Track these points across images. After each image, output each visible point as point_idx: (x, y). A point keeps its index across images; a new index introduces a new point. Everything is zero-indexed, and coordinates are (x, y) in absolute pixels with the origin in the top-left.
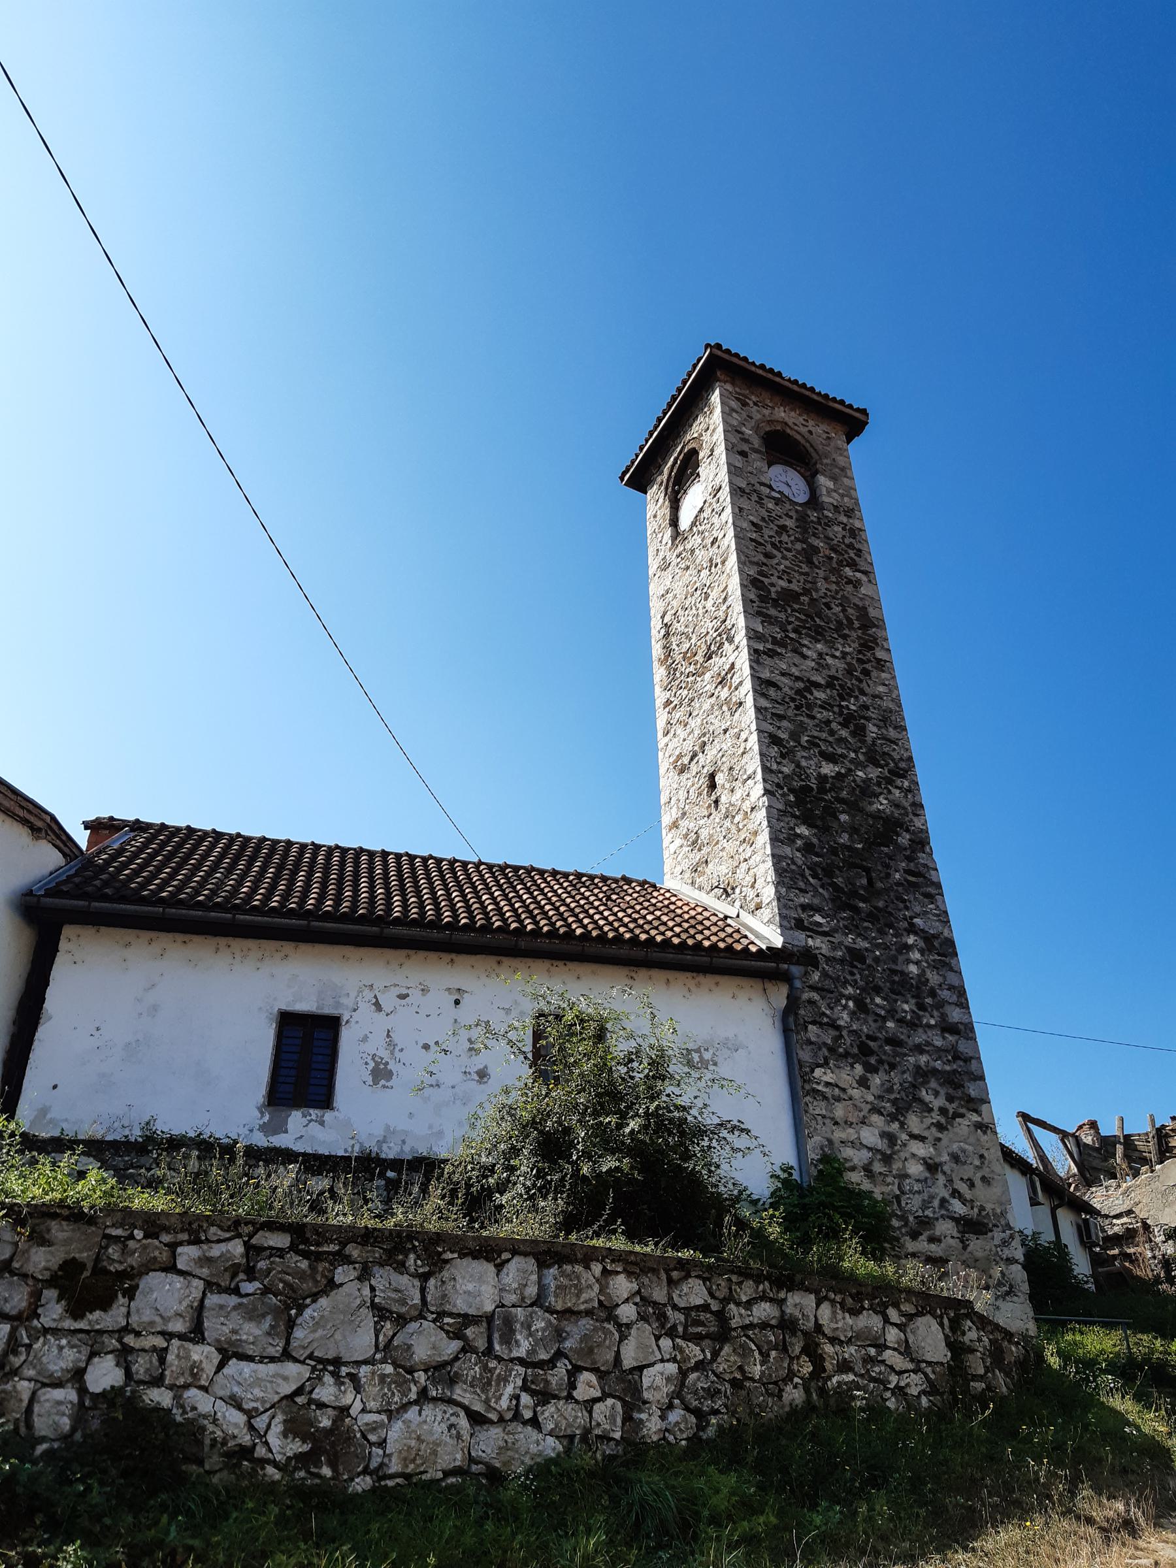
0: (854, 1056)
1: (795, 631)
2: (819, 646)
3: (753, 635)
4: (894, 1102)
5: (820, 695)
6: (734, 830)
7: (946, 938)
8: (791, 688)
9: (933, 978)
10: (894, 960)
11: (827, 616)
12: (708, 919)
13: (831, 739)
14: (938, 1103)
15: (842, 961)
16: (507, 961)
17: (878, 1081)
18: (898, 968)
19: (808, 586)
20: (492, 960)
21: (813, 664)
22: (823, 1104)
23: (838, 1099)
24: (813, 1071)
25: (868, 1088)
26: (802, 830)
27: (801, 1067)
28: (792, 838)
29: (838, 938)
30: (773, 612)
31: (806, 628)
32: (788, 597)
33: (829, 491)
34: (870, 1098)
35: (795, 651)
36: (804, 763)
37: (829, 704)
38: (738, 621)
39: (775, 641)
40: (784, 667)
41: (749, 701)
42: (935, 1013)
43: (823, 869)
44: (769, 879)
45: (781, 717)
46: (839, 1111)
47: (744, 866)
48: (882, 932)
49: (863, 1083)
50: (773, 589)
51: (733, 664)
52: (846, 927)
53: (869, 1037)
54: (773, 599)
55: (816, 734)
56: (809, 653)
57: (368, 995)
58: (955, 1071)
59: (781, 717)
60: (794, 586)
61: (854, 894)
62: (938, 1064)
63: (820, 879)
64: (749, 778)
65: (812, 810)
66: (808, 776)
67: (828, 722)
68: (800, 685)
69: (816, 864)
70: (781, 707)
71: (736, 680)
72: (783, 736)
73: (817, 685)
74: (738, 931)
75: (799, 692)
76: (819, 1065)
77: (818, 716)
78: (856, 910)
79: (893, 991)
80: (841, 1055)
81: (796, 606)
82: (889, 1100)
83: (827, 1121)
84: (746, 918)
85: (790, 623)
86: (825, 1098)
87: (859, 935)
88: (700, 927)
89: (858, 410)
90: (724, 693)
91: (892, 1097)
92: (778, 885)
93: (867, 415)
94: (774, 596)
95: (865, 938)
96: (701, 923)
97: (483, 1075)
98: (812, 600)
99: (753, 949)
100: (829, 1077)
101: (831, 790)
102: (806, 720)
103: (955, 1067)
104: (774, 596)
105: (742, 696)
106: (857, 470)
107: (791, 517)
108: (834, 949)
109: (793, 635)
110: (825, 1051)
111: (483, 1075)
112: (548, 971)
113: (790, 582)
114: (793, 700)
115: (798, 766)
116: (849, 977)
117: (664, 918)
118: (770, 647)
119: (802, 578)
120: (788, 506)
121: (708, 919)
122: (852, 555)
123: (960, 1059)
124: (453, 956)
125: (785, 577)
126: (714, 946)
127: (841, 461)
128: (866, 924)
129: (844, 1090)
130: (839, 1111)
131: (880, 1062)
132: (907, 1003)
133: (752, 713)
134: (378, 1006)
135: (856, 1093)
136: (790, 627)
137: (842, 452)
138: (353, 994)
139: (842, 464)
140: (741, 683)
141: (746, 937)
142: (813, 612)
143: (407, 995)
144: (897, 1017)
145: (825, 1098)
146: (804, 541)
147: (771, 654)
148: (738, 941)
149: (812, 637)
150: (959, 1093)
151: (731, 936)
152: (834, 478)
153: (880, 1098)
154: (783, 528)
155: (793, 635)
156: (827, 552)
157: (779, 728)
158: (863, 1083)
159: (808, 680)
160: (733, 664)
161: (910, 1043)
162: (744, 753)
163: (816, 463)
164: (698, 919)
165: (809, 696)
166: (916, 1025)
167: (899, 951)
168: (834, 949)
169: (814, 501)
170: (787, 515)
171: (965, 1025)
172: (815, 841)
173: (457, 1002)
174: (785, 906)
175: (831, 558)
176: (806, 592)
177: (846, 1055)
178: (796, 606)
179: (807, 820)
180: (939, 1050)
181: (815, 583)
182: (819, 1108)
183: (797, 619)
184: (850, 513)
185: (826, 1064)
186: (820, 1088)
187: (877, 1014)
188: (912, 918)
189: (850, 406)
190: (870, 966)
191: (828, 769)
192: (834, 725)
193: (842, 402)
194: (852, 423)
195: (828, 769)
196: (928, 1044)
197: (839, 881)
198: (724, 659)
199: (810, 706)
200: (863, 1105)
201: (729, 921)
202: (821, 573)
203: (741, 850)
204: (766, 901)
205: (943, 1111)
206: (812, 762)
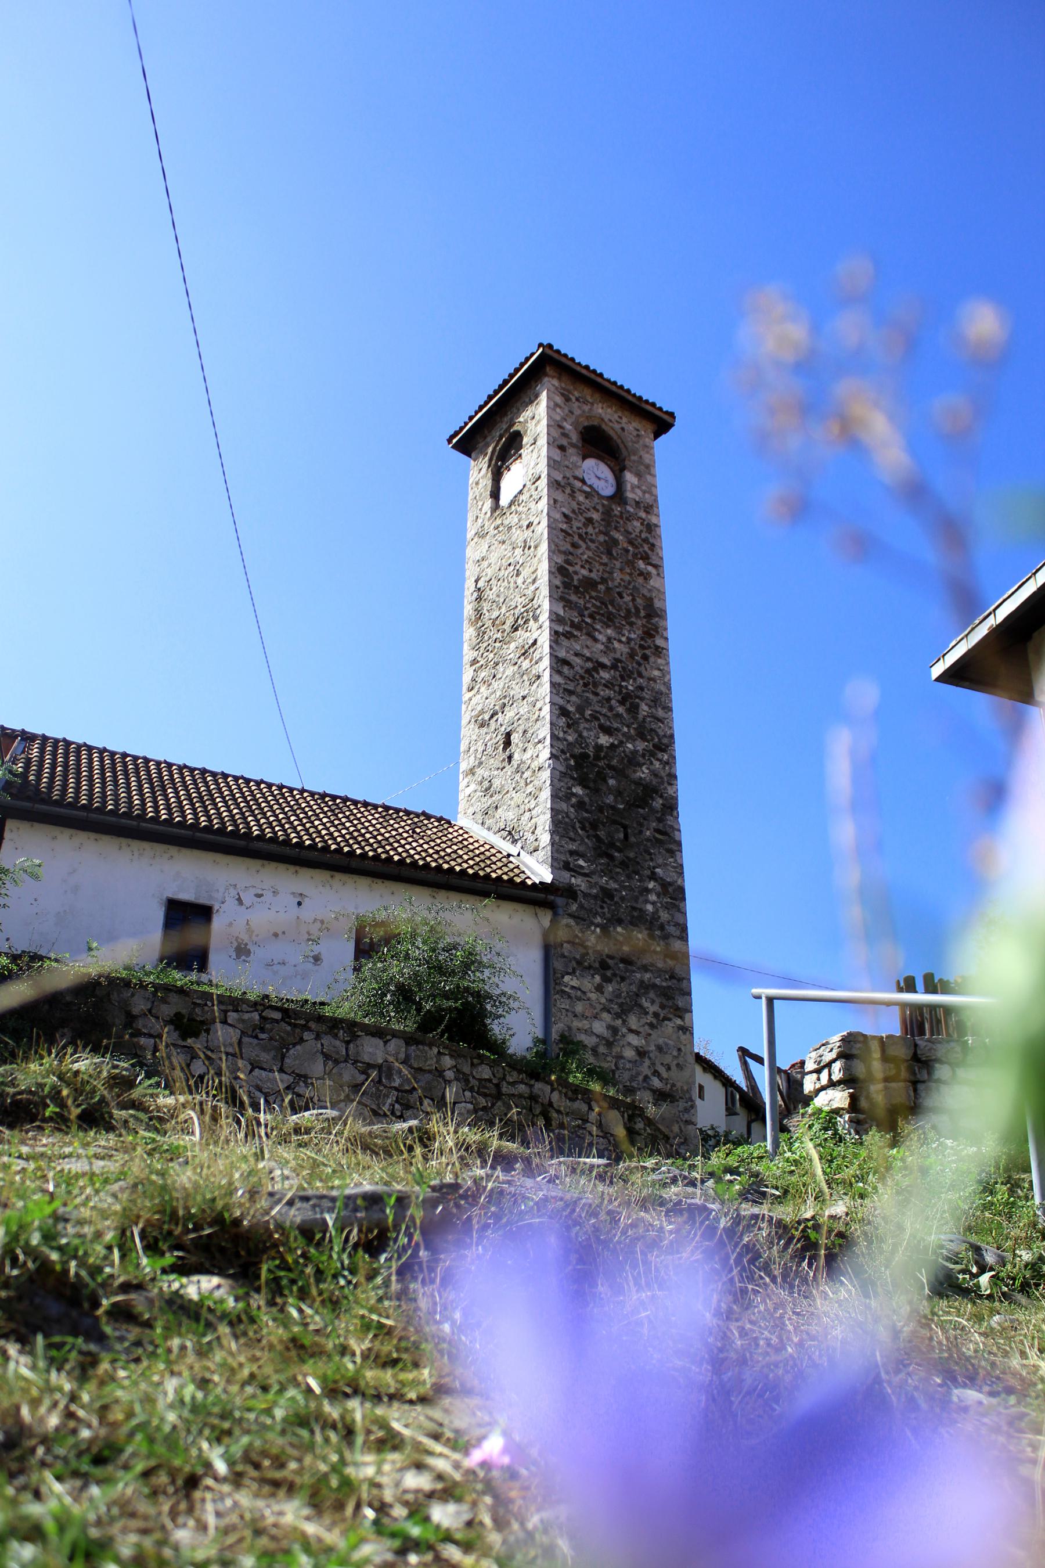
0: (595, 969)
1: (591, 616)
2: (609, 631)
3: (555, 618)
4: (621, 1005)
5: (605, 675)
6: (522, 784)
8: (582, 668)
11: (619, 605)
12: (494, 855)
13: (609, 714)
14: (653, 1008)
15: (595, 897)
16: (338, 876)
17: (610, 989)
18: (639, 906)
19: (606, 575)
20: (326, 874)
21: (602, 647)
22: (568, 1001)
23: (579, 999)
24: (563, 977)
25: (602, 993)
26: (578, 790)
27: (555, 973)
28: (569, 796)
29: (595, 879)
30: (573, 598)
31: (599, 614)
32: (589, 584)
33: (633, 487)
34: (603, 1000)
35: (589, 634)
36: (585, 734)
37: (612, 684)
38: (546, 605)
39: (573, 625)
40: (578, 648)
41: (546, 677)
43: (590, 824)
44: (547, 828)
45: (571, 693)
46: (579, 1008)
47: (527, 815)
48: (629, 877)
49: (599, 989)
50: (576, 577)
51: (535, 641)
52: (602, 871)
53: (608, 956)
54: (575, 587)
55: (598, 709)
56: (600, 637)
57: (233, 892)
58: (669, 987)
59: (571, 693)
60: (593, 575)
61: (612, 845)
62: (658, 981)
63: (587, 831)
64: (539, 742)
65: (587, 774)
66: (587, 745)
67: (609, 699)
68: (589, 665)
69: (585, 819)
70: (572, 684)
71: (537, 656)
72: (571, 709)
73: (603, 666)
74: (517, 867)
75: (588, 671)
76: (568, 974)
77: (602, 693)
78: (611, 858)
80: (586, 968)
81: (594, 594)
82: (617, 1003)
83: (569, 1014)
84: (525, 857)
85: (587, 609)
86: (570, 997)
87: (611, 878)
88: (488, 862)
89: (667, 413)
90: (526, 664)
91: (620, 1001)
92: (553, 833)
93: (674, 418)
94: (576, 583)
95: (616, 881)
96: (489, 858)
97: (317, 959)
98: (608, 589)
99: (529, 882)
100: (575, 983)
101: (605, 757)
102: (591, 696)
103: (670, 984)
104: (576, 583)
105: (541, 670)
106: (659, 469)
107: (598, 511)
108: (591, 887)
109: (588, 620)
110: (574, 963)
111: (317, 959)
112: (370, 886)
113: (591, 571)
114: (582, 678)
115: (580, 735)
117: (460, 852)
118: (568, 629)
119: (601, 568)
120: (596, 500)
121: (494, 855)
122: (646, 549)
124: (298, 868)
125: (587, 566)
126: (499, 878)
127: (647, 458)
128: (618, 870)
129: (584, 993)
130: (579, 1008)
131: (615, 975)
132: (641, 932)
133: (547, 687)
134: (240, 901)
135: (593, 996)
136: (586, 613)
137: (648, 448)
138: (222, 890)
139: (647, 461)
140: (541, 659)
141: (523, 872)
142: (607, 593)
143: (262, 895)
145: (570, 997)
146: (606, 534)
147: (568, 635)
148: (517, 875)
149: (604, 623)
151: (512, 870)
152: (639, 475)
153: (611, 1001)
154: (590, 521)
155: (588, 620)
156: (625, 545)
157: (569, 702)
158: (599, 989)
159: (597, 662)
160: (535, 641)
161: (639, 963)
162: (537, 720)
163: (624, 460)
164: (487, 854)
165: (596, 675)
168: (591, 887)
169: (619, 496)
170: (594, 508)
172: (586, 799)
173: (299, 904)
174: (557, 851)
175: (627, 551)
176: (604, 581)
177: (590, 967)
178: (594, 594)
179: (583, 782)
181: (611, 573)
182: (564, 1004)
183: (594, 605)
184: (649, 508)
185: (573, 973)
186: (567, 989)
187: (616, 940)
189: (660, 409)
190: (616, 903)
191: (604, 740)
192: (613, 702)
193: (653, 405)
194: (661, 423)
195: (604, 740)
196: (652, 965)
197: (601, 834)
198: (528, 634)
199: (595, 685)
200: (597, 1005)
201: (511, 859)
202: (618, 564)
203: (526, 801)
204: (542, 845)
205: (656, 1015)
206: (592, 733)
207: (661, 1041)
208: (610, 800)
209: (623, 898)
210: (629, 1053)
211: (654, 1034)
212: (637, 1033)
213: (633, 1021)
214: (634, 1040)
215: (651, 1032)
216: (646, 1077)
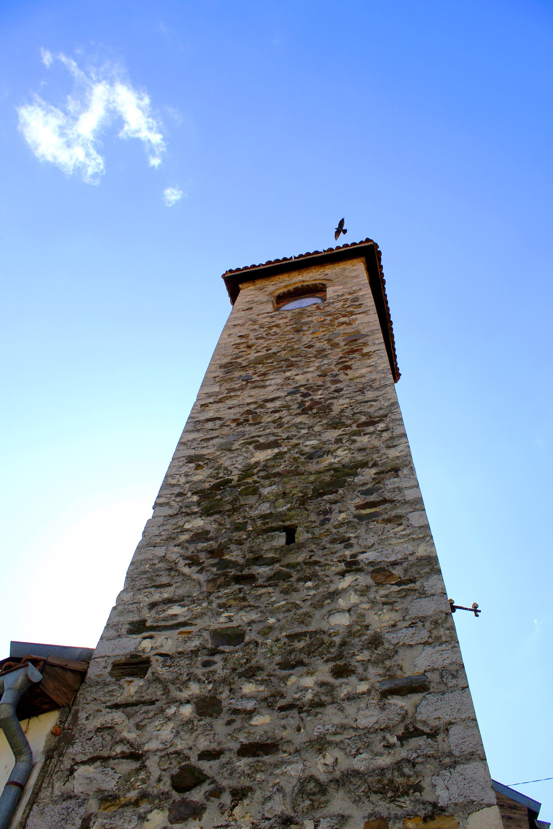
7: (420, 559)
9: (380, 620)
42: (373, 672)
79: (284, 666)
132: (310, 673)
144: (282, 702)
150: (407, 803)
161: (300, 739)
166: (322, 705)
167: (318, 605)
171: (443, 672)
180: (369, 731)
187: (236, 712)
188: (354, 556)
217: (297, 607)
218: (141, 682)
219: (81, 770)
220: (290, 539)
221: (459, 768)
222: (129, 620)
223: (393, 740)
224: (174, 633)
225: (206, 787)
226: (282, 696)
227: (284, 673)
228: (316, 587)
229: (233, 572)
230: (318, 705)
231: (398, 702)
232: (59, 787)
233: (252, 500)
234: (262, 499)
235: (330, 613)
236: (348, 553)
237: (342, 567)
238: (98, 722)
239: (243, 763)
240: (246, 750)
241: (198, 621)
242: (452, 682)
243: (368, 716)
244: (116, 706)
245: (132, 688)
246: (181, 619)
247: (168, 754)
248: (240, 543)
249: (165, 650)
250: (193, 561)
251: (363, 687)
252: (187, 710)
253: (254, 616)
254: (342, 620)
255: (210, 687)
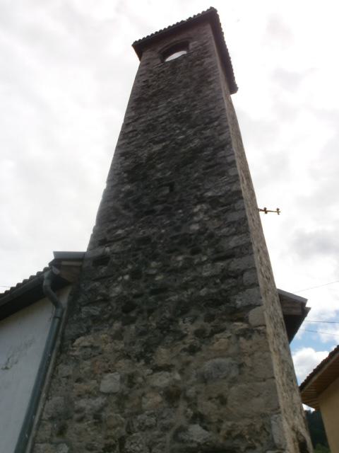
9: (212, 225)
10: (178, 229)
42: (209, 251)
78: (153, 212)
79: (168, 252)
116: (131, 259)
123: (230, 277)
144: (168, 269)
161: (177, 284)
166: (186, 269)
180: (207, 278)
207: (207, 366)
208: (159, 175)
209: (161, 237)
210: (153, 400)
211: (194, 360)
212: (168, 368)
213: (162, 355)
214: (162, 380)
215: (191, 358)
216: (182, 429)
217: (174, 223)
218: (106, 268)
219: (84, 309)
220: (171, 190)
221: (247, 290)
222: (100, 238)
223: (218, 281)
224: (120, 243)
225: (137, 310)
226: (168, 266)
227: (168, 255)
228: (184, 212)
229: (145, 210)
230: (184, 269)
231: (220, 264)
232: (75, 317)
233: (152, 172)
234: (158, 171)
235: (190, 224)
236: (199, 193)
237: (196, 201)
238: (89, 288)
239: (151, 298)
240: (153, 292)
241: (131, 236)
242: (246, 252)
243: (207, 272)
244: (97, 280)
245: (103, 270)
246: (122, 236)
247: (121, 298)
248: (147, 195)
249: (115, 251)
250: (126, 207)
251: (205, 258)
252: (127, 277)
253: (155, 230)
254: (195, 227)
255: (137, 265)
